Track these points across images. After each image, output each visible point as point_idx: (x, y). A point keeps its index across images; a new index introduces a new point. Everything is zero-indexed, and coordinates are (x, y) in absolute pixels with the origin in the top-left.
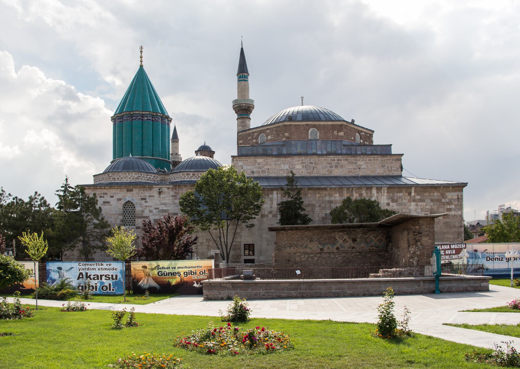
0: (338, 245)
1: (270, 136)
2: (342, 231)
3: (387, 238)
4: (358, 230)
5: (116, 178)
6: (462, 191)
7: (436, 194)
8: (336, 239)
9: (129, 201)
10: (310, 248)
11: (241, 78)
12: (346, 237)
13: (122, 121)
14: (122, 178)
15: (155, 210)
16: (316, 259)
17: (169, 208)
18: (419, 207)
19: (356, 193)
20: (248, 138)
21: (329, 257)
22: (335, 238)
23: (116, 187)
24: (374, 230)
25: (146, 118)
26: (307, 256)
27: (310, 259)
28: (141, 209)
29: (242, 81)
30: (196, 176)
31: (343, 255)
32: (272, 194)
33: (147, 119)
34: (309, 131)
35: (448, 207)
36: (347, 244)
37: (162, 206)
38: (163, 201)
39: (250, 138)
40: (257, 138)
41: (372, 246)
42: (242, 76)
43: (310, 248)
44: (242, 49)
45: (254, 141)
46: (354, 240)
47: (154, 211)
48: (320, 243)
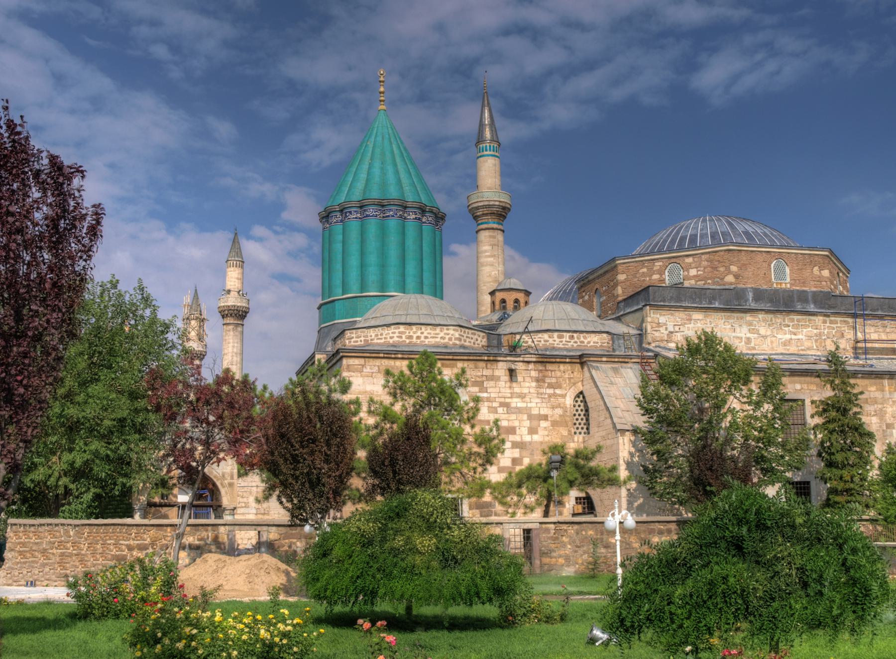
5: (415, 336)
11: (486, 150)
13: (360, 218)
14: (426, 337)
15: (502, 408)
17: (529, 405)
20: (641, 271)
23: (393, 356)
25: (414, 216)
29: (490, 157)
30: (576, 340)
34: (772, 265)
37: (515, 400)
38: (517, 390)
40: (661, 273)
42: (490, 146)
45: (656, 277)
47: (500, 410)
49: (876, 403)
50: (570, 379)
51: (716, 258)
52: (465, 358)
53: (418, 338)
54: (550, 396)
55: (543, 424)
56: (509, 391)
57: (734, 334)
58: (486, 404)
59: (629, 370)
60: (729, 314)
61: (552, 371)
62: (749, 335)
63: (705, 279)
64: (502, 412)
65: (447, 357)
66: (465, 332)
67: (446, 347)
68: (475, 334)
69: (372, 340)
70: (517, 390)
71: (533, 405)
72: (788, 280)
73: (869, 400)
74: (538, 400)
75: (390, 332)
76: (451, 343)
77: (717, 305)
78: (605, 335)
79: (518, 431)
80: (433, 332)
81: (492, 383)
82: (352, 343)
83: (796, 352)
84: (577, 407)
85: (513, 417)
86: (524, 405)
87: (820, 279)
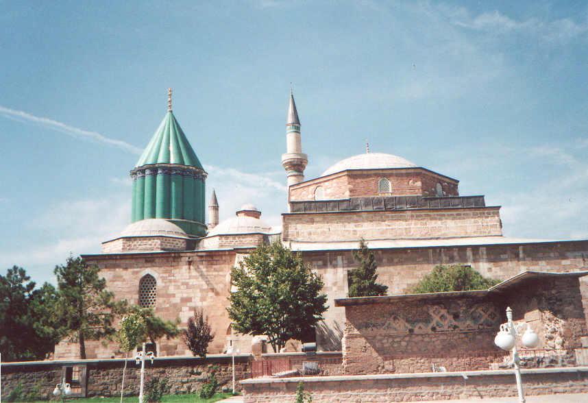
0: (433, 323)
2: (438, 304)
4: (459, 302)
10: (395, 329)
12: (443, 312)
14: (140, 245)
19: (446, 255)
21: (423, 341)
26: (390, 340)
27: (396, 345)
28: (164, 285)
31: (441, 337)
32: (336, 259)
36: (446, 322)
37: (192, 280)
39: (304, 192)
41: (482, 325)
43: (395, 329)
46: (456, 317)
47: (182, 287)
48: (407, 321)
51: (341, 181)
53: (135, 245)
54: (215, 276)
56: (187, 274)
61: (217, 261)
62: (355, 229)
66: (166, 240)
72: (391, 191)
79: (193, 300)
86: (197, 283)
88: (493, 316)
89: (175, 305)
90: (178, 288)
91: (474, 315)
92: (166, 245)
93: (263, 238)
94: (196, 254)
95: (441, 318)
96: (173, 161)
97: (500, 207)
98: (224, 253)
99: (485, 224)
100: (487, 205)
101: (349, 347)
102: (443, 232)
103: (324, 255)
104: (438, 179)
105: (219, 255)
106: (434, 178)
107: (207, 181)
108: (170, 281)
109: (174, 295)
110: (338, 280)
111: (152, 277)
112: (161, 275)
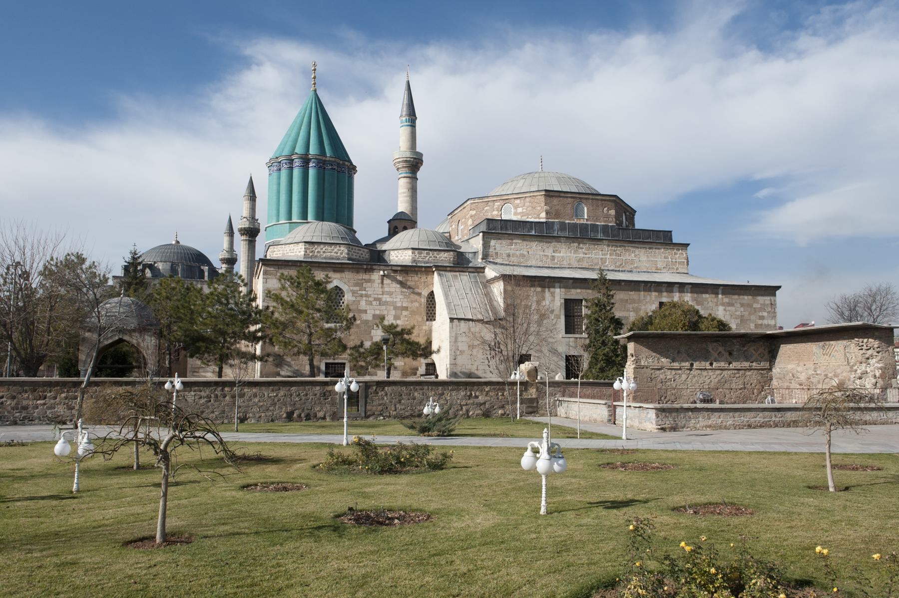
1: (521, 208)
2: (715, 341)
3: (769, 352)
4: (734, 341)
6: (775, 295)
7: (746, 297)
8: (708, 351)
9: (337, 286)
12: (721, 349)
14: (324, 252)
15: (375, 302)
16: (684, 377)
17: (395, 300)
18: (728, 313)
22: (708, 350)
24: (753, 341)
25: (331, 167)
26: (673, 372)
28: (354, 299)
33: (332, 169)
35: (760, 314)
37: (385, 296)
44: (408, 83)
45: (495, 213)
47: (374, 303)
49: (634, 303)
50: (425, 282)
51: (536, 200)
52: (350, 266)
55: (405, 313)
56: (381, 290)
57: (542, 253)
58: (364, 298)
59: (465, 277)
60: (540, 239)
62: (553, 254)
63: (528, 215)
64: (375, 304)
65: (337, 266)
66: (352, 249)
67: (338, 259)
68: (360, 250)
69: (287, 253)
70: (387, 289)
71: (398, 300)
72: (586, 217)
73: (629, 301)
74: (401, 297)
75: (299, 248)
76: (342, 256)
77: (533, 233)
78: (452, 253)
80: (329, 248)
81: (369, 284)
82: (274, 255)
83: (587, 267)
84: (429, 302)
85: (384, 307)
86: (391, 300)
87: (608, 216)
88: (762, 355)
89: (366, 322)
90: (370, 303)
91: (746, 353)
92: (352, 255)
93: (457, 255)
94: (390, 268)
95: (718, 354)
96: (328, 153)
97: (689, 244)
98: (420, 269)
99: (674, 260)
100: (674, 241)
101: (637, 378)
102: (635, 266)
103: (543, 281)
104: (624, 208)
105: (415, 271)
106: (621, 206)
107: (357, 178)
108: (362, 296)
109: (365, 312)
110: (555, 308)
111: (340, 289)
112: (351, 288)
